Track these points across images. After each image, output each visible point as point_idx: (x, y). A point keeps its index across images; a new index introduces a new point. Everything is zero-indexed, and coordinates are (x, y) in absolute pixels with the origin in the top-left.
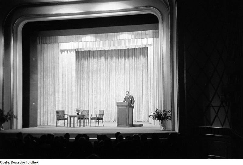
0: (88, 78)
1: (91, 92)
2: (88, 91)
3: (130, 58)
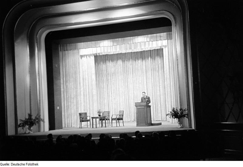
0: (107, 80)
2: (108, 94)
3: (147, 60)
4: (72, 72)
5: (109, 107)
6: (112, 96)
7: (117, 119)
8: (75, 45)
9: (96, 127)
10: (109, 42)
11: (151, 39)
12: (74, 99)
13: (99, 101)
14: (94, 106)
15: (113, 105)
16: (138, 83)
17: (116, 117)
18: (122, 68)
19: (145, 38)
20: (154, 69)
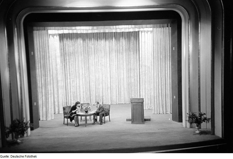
0: (64, 61)
1: (68, 76)
5: (66, 90)
15: (71, 87)
16: (100, 65)
18: (82, 48)
20: (118, 51)
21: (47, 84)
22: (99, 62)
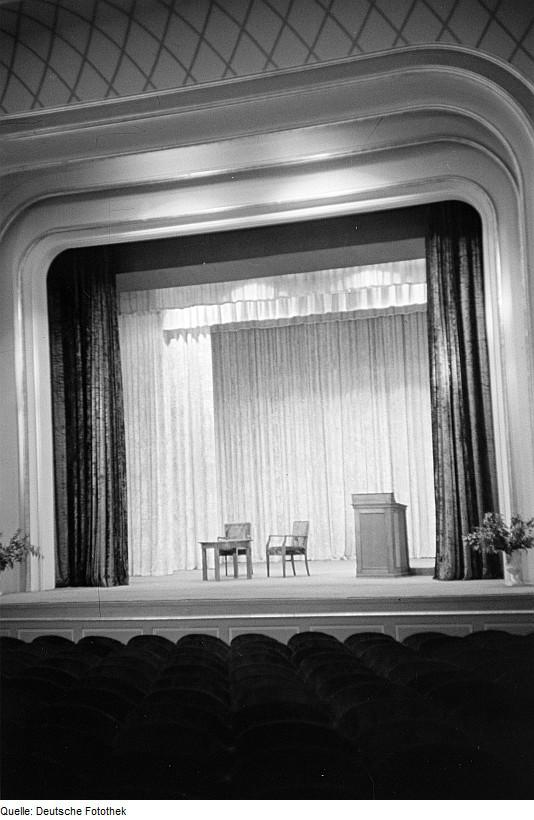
0: (254, 418)
1: (264, 464)
2: (256, 463)
4: (135, 389)
5: (258, 507)
6: (269, 471)
7: (284, 551)
8: (148, 293)
9: (217, 578)
10: (264, 287)
11: (406, 275)
12: (141, 480)
13: (225, 489)
14: (210, 506)
16: (358, 428)
17: (281, 545)
19: (387, 274)
21: (154, 467)
22: (354, 418)
